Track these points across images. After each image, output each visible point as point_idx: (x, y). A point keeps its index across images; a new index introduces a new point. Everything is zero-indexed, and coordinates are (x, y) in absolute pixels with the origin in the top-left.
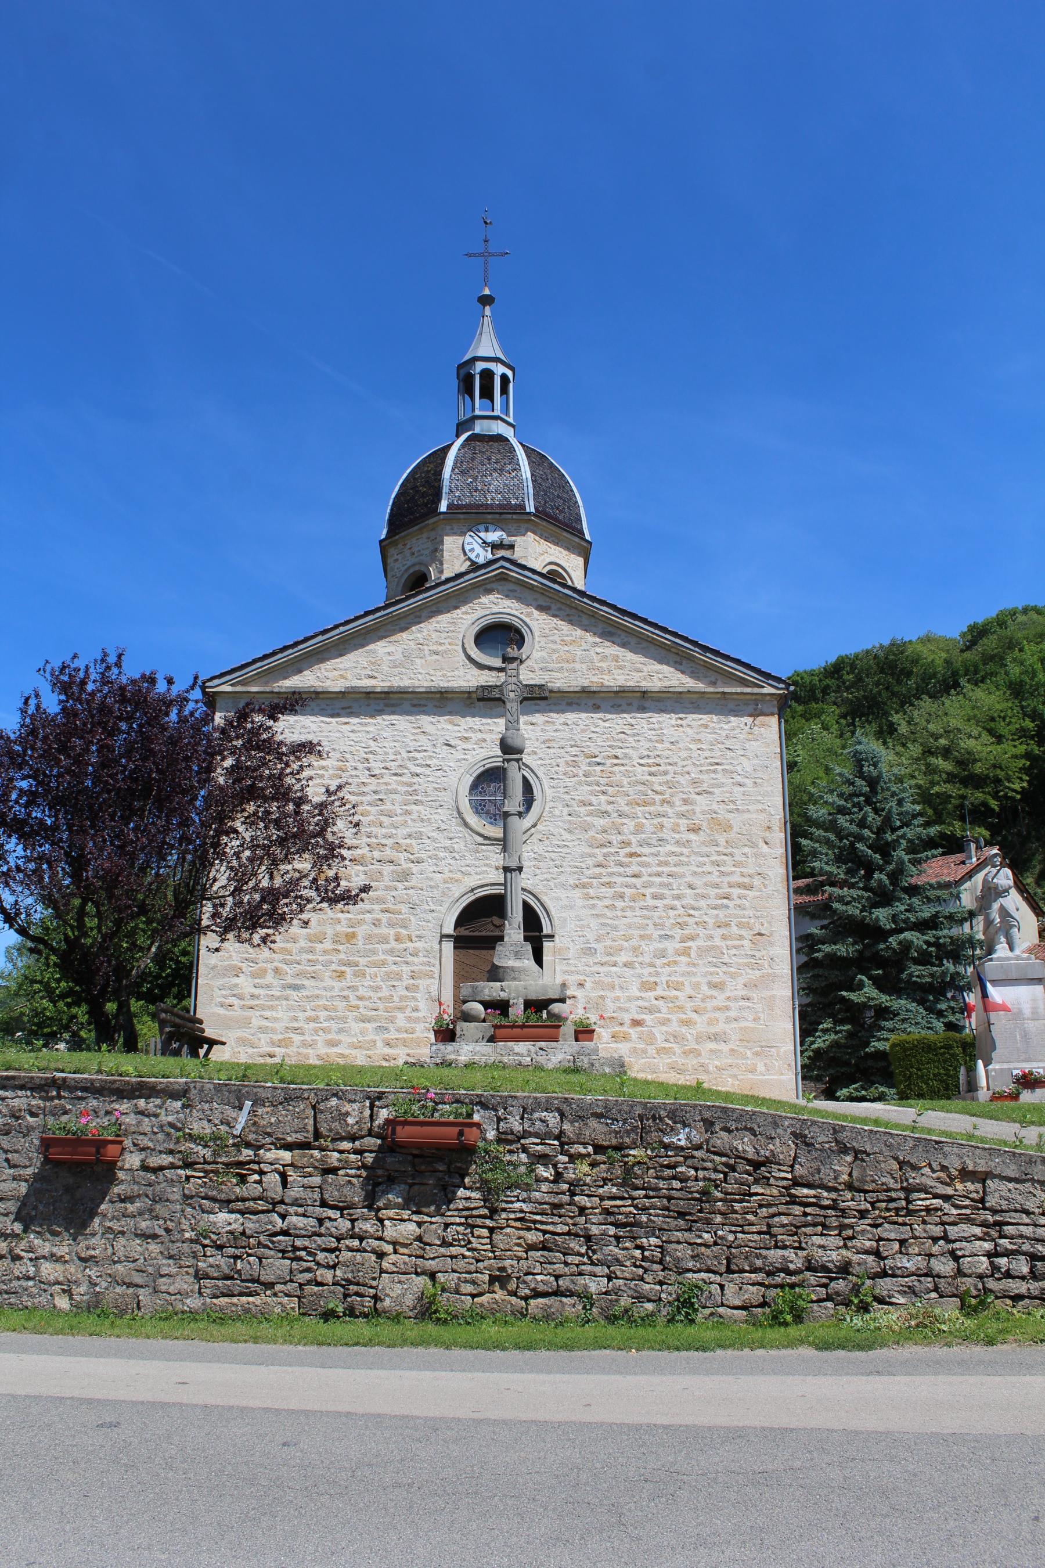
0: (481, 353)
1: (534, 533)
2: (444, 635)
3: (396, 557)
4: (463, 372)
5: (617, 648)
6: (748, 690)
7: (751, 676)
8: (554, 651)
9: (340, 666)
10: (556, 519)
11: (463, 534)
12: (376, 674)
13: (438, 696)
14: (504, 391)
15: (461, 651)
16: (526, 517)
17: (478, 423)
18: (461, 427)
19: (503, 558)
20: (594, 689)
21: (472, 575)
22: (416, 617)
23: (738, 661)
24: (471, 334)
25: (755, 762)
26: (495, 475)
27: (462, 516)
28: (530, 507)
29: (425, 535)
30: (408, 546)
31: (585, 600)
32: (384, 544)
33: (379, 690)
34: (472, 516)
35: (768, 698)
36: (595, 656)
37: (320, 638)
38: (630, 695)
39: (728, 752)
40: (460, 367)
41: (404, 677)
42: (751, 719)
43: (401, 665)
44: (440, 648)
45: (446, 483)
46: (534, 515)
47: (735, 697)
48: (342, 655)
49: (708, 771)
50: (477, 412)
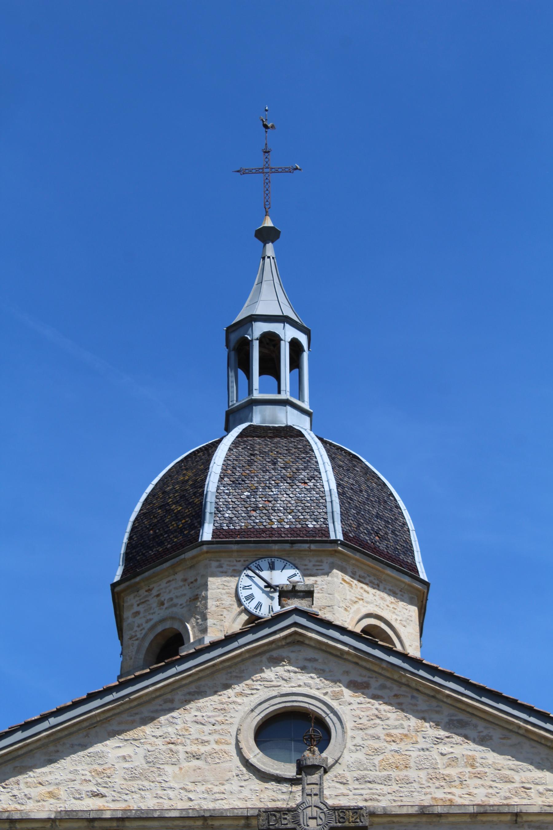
0: (260, 310)
1: (343, 570)
2: (208, 728)
3: (136, 609)
4: (234, 337)
5: (472, 746)
8: (377, 751)
9: (50, 778)
10: (376, 550)
11: (237, 573)
12: (103, 791)
13: (199, 823)
14: (295, 363)
15: (234, 752)
16: (329, 547)
18: (232, 417)
19: (297, 611)
20: (439, 810)
21: (250, 637)
22: (166, 702)
24: (246, 284)
26: (284, 485)
27: (235, 547)
28: (336, 532)
29: (180, 576)
30: (154, 592)
31: (422, 673)
32: (118, 589)
33: (108, 815)
34: (250, 547)
36: (438, 758)
37: (19, 735)
38: (495, 818)
40: (230, 330)
41: (147, 794)
43: (143, 776)
44: (203, 749)
45: (211, 498)
46: (343, 544)
48: (51, 761)
50: (256, 395)
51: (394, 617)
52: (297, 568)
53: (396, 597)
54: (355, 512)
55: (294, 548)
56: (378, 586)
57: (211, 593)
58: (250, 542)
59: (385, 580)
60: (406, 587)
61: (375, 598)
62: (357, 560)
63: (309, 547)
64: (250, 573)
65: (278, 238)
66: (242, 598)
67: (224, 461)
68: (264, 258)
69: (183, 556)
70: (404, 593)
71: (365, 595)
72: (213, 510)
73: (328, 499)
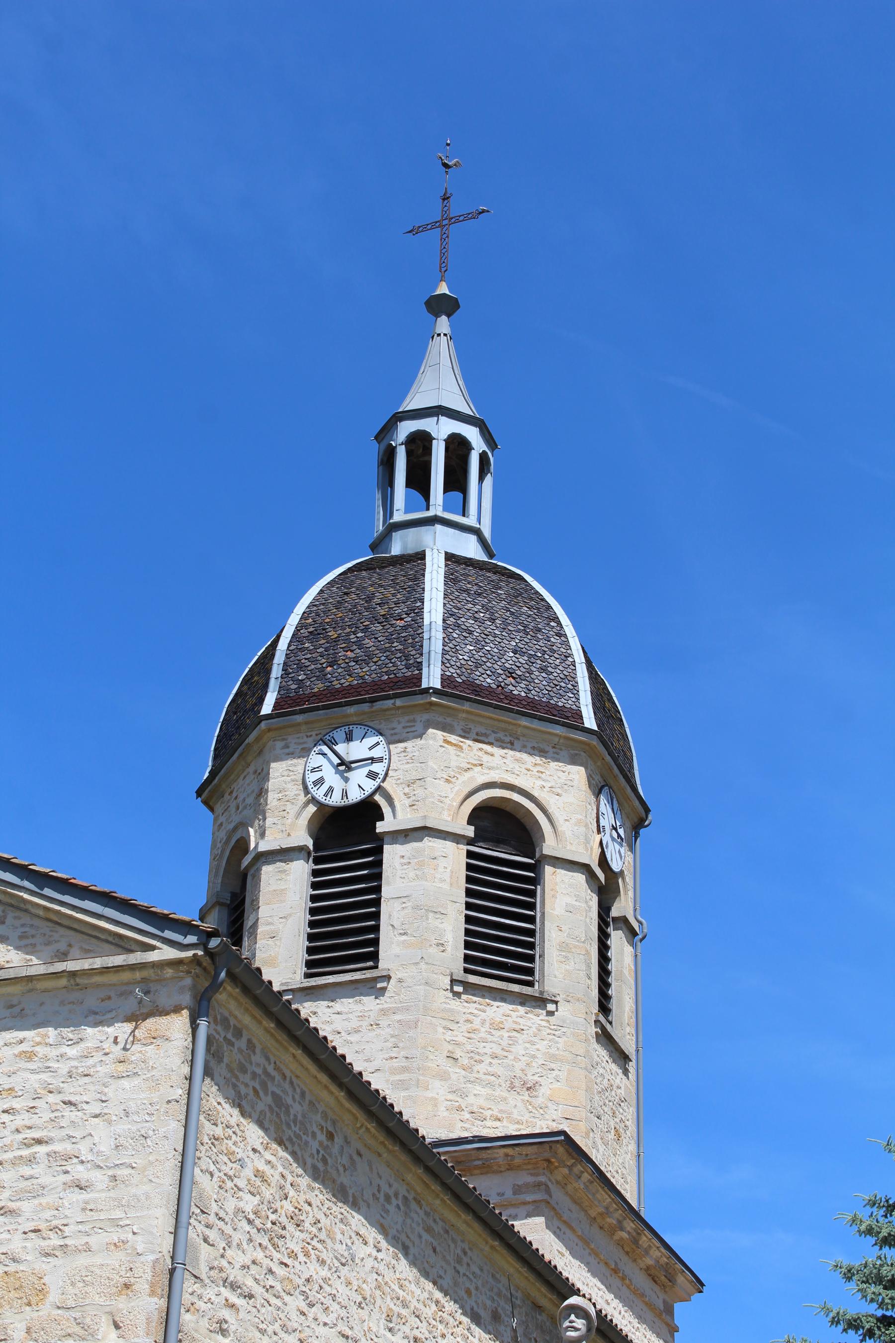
1: (444, 728)
6: (119, 960)
7: (127, 926)
16: (419, 700)
17: (397, 536)
23: (106, 898)
25: (122, 1127)
27: (299, 718)
28: (432, 678)
29: (251, 769)
30: (234, 795)
35: (169, 972)
39: (67, 1111)
42: (128, 1027)
47: (98, 979)
49: (17, 1161)
51: (539, 783)
52: (381, 734)
53: (546, 758)
54: (472, 648)
55: (374, 708)
56: (512, 744)
57: (272, 784)
58: (317, 709)
59: (524, 736)
60: (561, 741)
61: (505, 761)
62: (468, 712)
63: (394, 704)
64: (325, 749)
65: (458, 307)
66: (309, 784)
67: (308, 607)
68: (433, 337)
69: (247, 742)
70: (561, 750)
71: (486, 758)
72: (280, 673)
73: (426, 636)
